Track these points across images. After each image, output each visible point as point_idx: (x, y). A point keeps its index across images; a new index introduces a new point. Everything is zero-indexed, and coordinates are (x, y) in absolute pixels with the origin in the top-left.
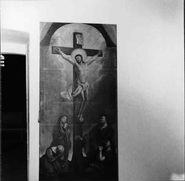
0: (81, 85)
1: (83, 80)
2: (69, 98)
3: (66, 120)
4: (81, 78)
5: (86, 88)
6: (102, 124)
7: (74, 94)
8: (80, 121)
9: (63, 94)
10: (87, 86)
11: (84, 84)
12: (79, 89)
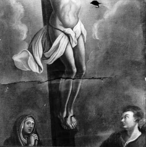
0: (63, 32)
1: (70, 19)
2: (35, 69)
3: (32, 126)
4: (63, 14)
5: (78, 39)
6: (126, 133)
7: (48, 58)
8: (68, 126)
9: (21, 59)
10: (82, 34)
11: (72, 29)
12: (59, 44)
